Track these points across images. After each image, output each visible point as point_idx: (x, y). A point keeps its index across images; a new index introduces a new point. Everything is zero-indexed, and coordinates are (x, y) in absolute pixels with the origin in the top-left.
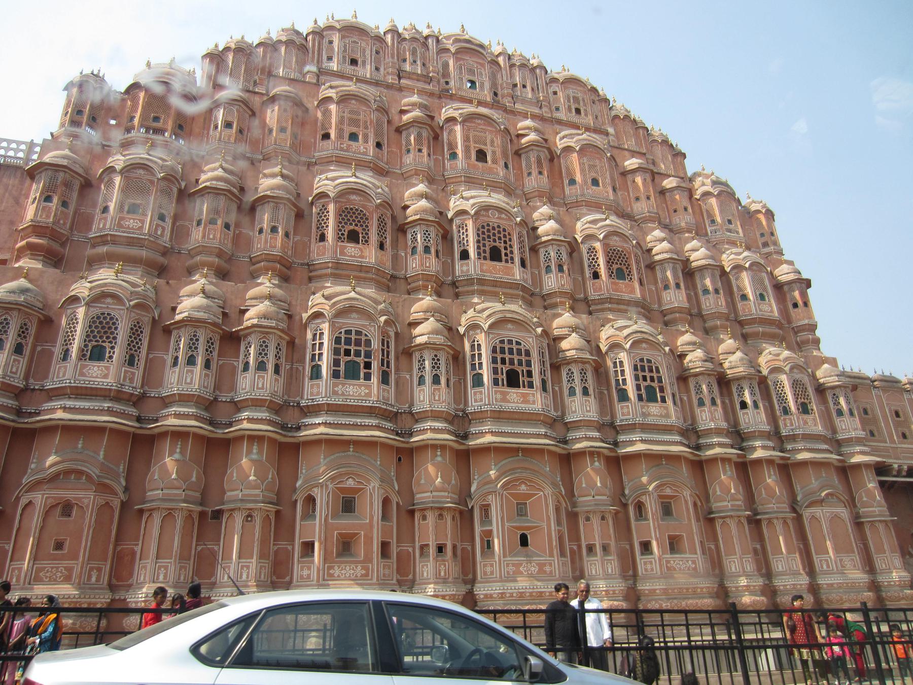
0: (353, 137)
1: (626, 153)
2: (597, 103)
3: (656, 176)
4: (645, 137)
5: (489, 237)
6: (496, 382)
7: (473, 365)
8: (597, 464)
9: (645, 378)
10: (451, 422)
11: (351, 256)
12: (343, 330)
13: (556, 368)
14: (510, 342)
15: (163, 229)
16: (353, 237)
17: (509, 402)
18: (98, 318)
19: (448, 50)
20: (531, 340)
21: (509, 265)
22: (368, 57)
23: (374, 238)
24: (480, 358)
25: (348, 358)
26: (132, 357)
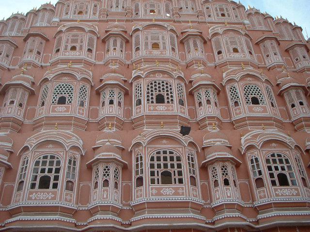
0: (74, 48)
1: (259, 32)
3: (280, 42)
4: (271, 22)
5: (156, 89)
6: (153, 181)
7: (137, 173)
9: (276, 168)
10: (119, 216)
12: (42, 157)
13: (204, 168)
14: (165, 152)
16: (62, 101)
17: (162, 195)
21: (170, 104)
24: (141, 166)
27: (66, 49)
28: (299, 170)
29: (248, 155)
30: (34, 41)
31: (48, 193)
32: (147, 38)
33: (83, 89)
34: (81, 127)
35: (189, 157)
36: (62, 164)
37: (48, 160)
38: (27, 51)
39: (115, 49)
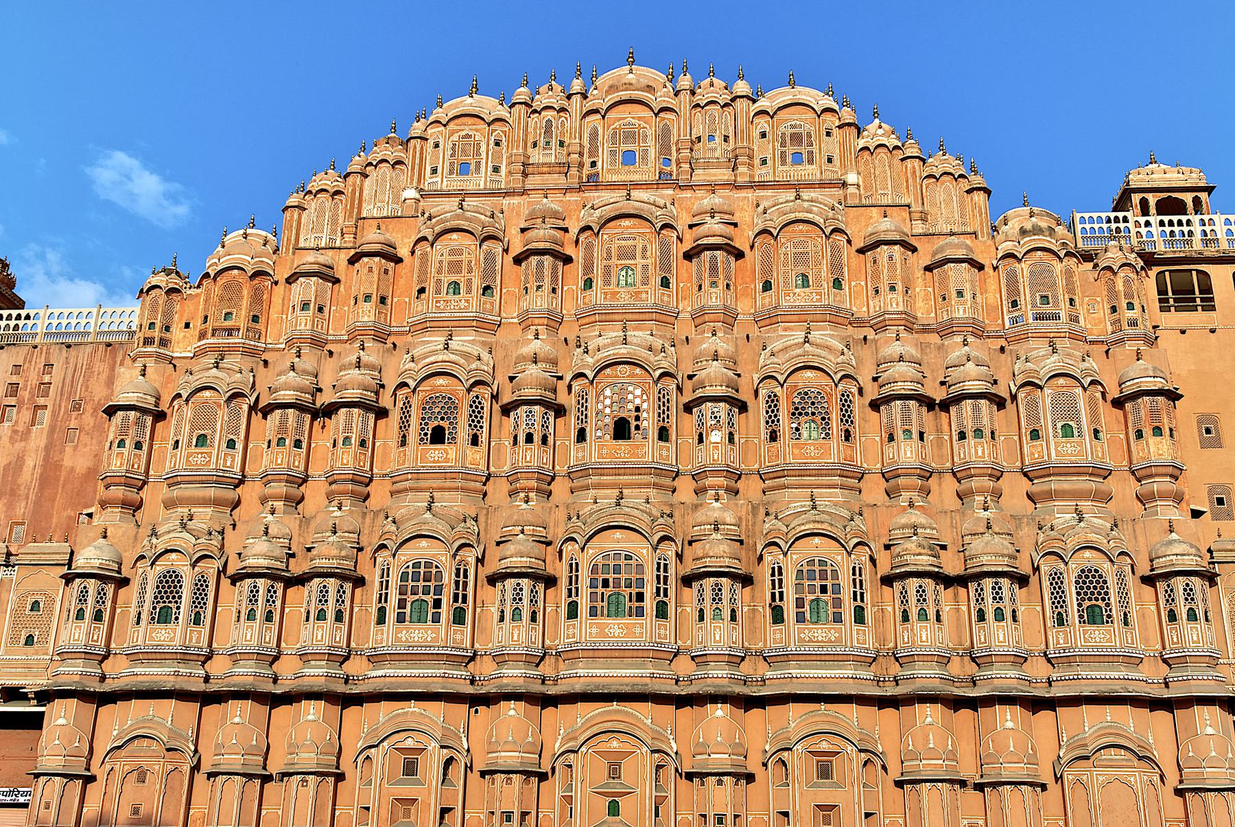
0: (455, 287)
2: (835, 131)
6: (593, 612)
7: (570, 591)
8: (719, 713)
11: (434, 462)
12: (410, 564)
15: (233, 457)
16: (438, 436)
18: (165, 577)
19: (596, 111)
20: (645, 551)
22: (484, 155)
23: (463, 433)
25: (416, 597)
26: (198, 614)
27: (438, 292)
28: (855, 593)
29: (768, 558)
30: (370, 270)
31: (426, 630)
32: (609, 257)
33: (476, 408)
34: (475, 491)
35: (659, 564)
36: (446, 580)
37: (422, 570)
38: (361, 298)
39: (539, 287)
